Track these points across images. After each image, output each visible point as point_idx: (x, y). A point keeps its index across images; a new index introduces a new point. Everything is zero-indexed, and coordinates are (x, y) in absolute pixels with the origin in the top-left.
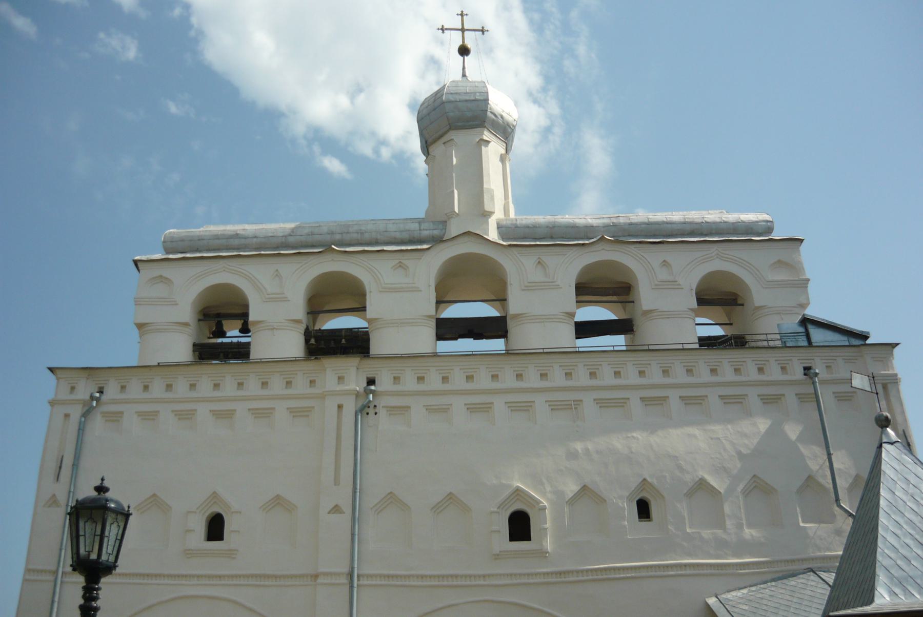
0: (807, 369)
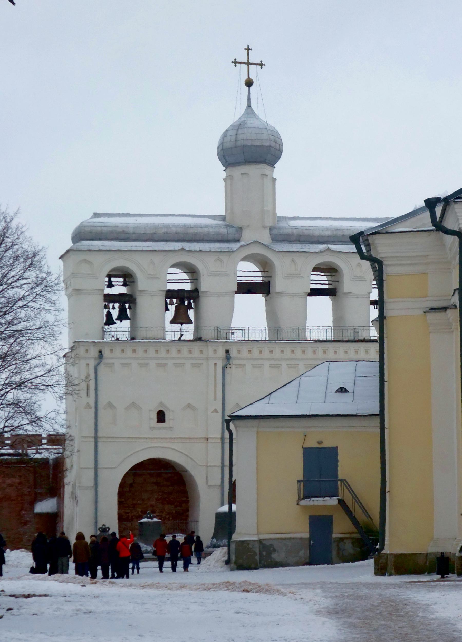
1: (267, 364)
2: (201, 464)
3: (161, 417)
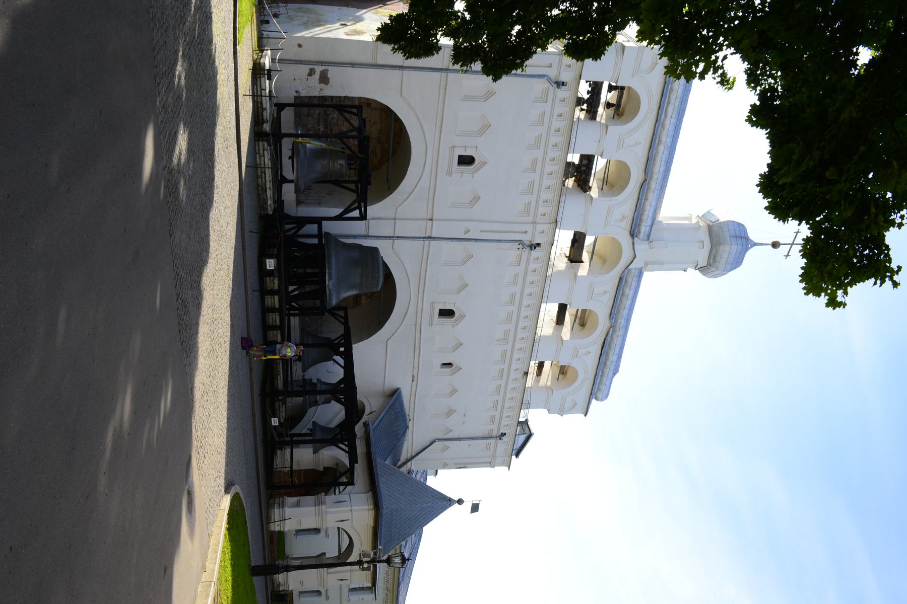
0: (504, 434)
1: (517, 289)
2: (398, 210)
3: (466, 160)
